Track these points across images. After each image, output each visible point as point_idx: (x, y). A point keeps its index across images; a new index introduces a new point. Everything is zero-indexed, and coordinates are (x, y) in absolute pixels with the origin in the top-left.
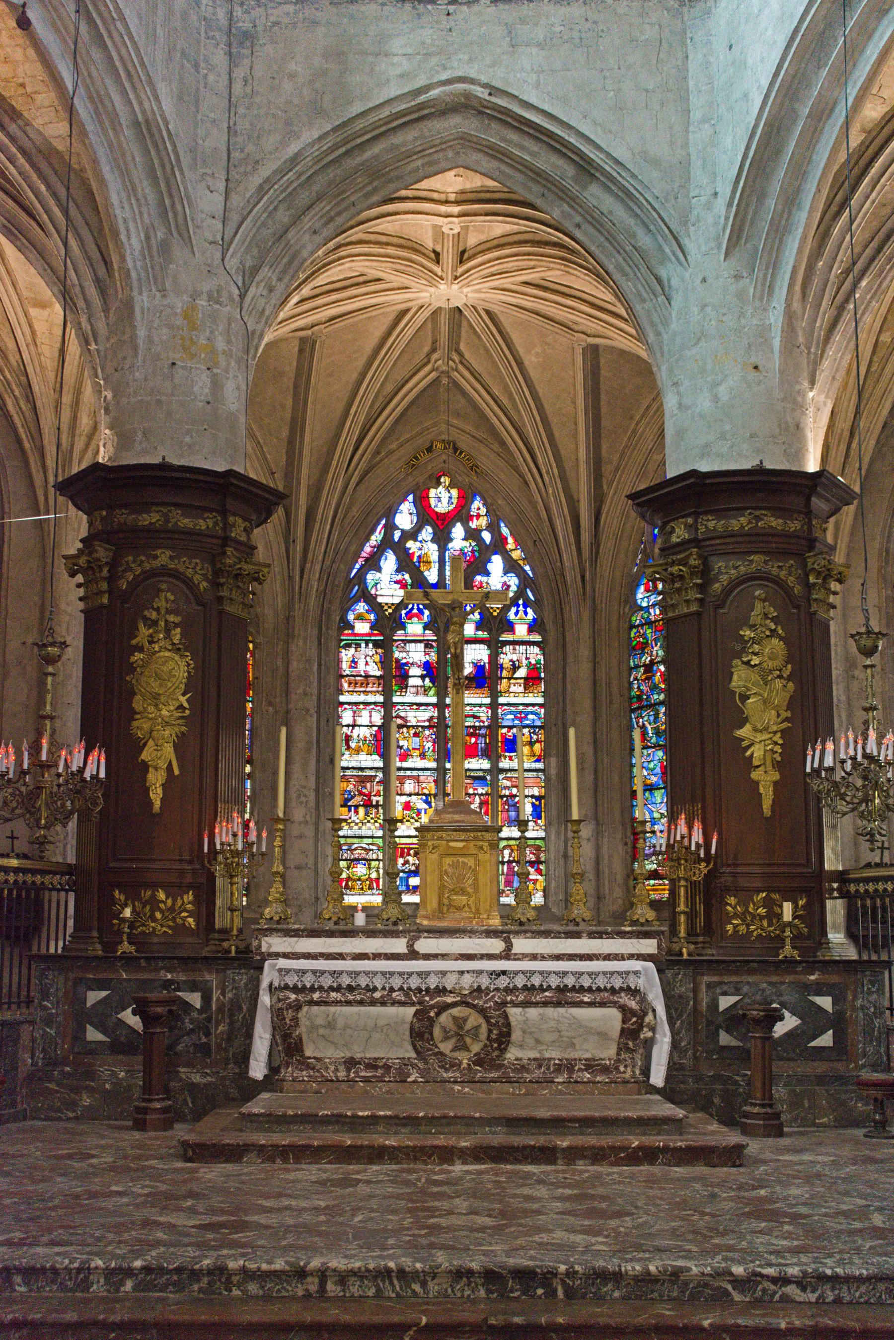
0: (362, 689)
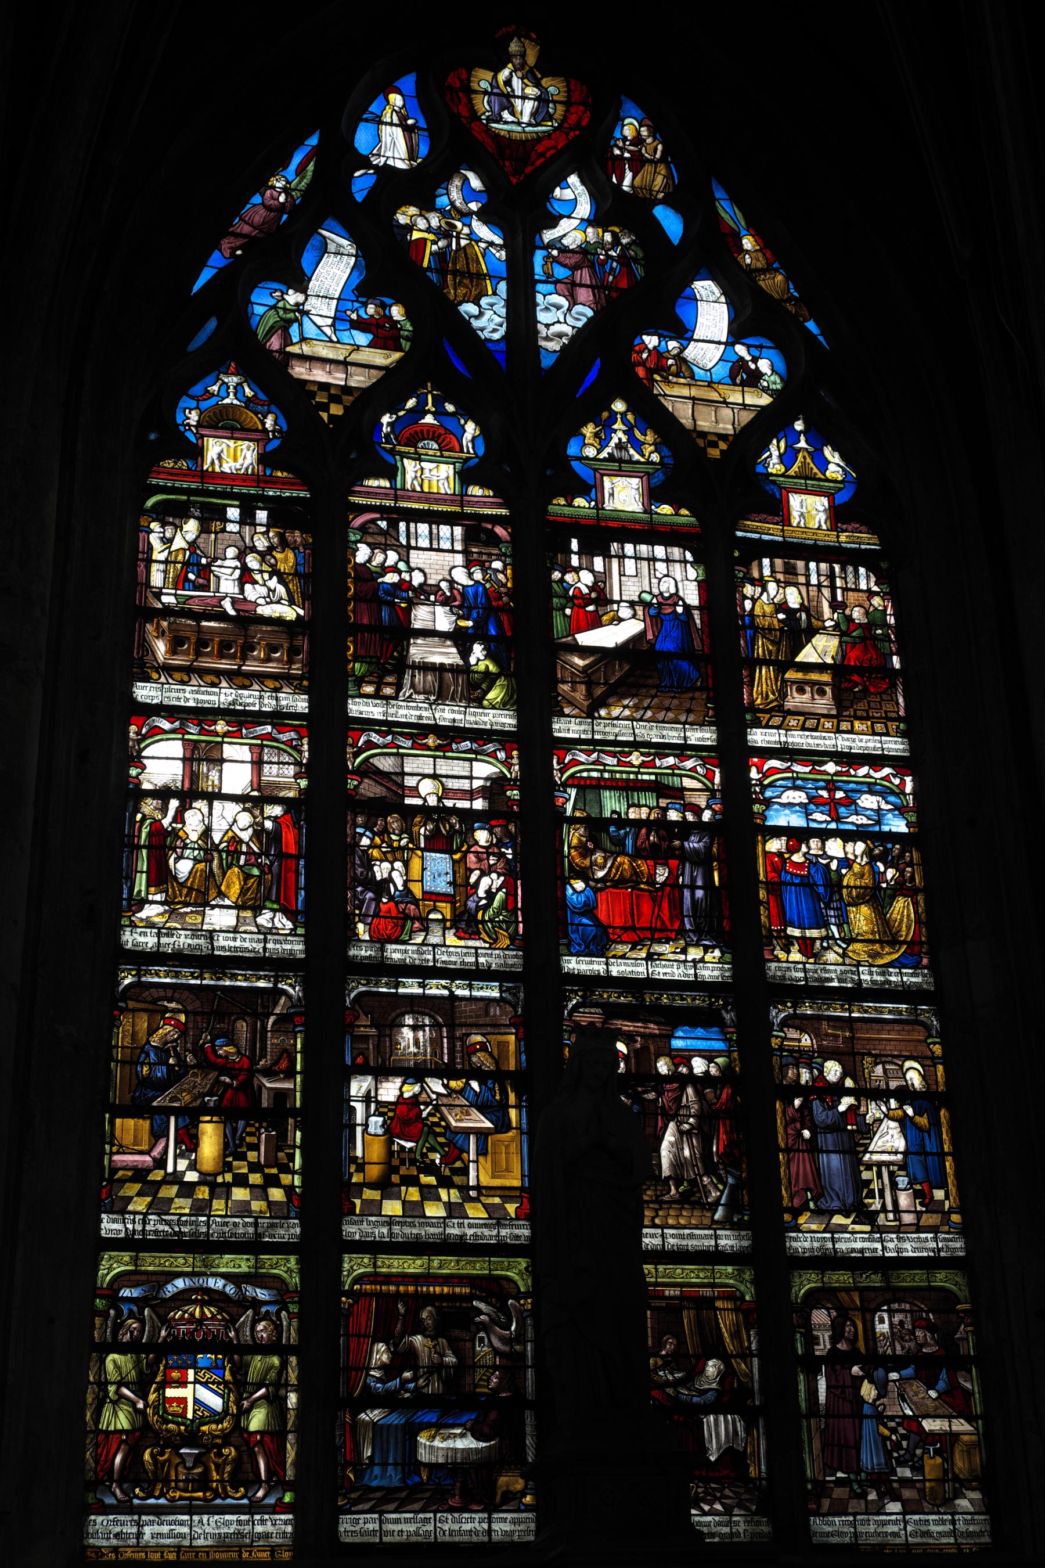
0: (224, 665)
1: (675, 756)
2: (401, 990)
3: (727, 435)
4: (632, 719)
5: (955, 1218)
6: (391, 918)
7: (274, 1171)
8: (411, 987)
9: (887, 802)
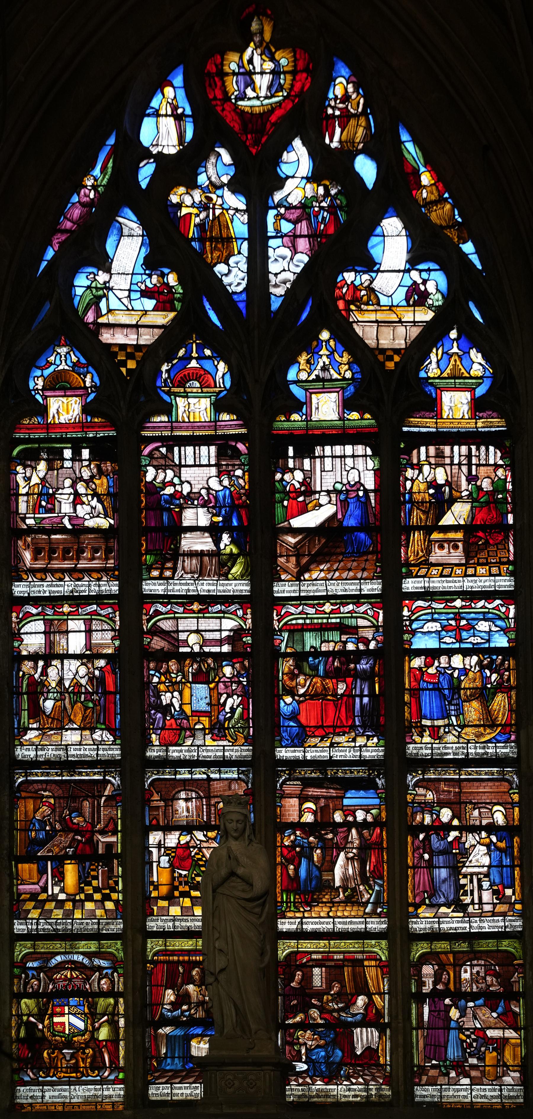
1: (353, 603)
2: (178, 777)
3: (400, 349)
4: (326, 579)
5: (518, 907)
6: (173, 729)
7: (108, 891)
8: (184, 775)
9: (496, 626)
